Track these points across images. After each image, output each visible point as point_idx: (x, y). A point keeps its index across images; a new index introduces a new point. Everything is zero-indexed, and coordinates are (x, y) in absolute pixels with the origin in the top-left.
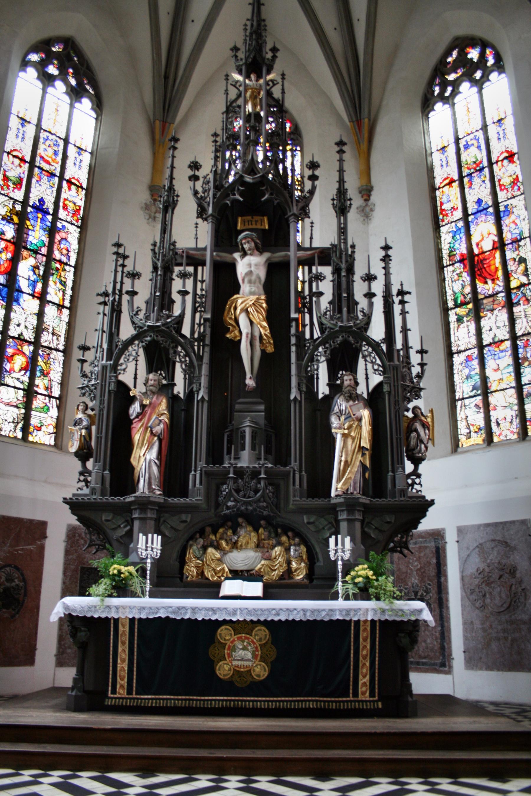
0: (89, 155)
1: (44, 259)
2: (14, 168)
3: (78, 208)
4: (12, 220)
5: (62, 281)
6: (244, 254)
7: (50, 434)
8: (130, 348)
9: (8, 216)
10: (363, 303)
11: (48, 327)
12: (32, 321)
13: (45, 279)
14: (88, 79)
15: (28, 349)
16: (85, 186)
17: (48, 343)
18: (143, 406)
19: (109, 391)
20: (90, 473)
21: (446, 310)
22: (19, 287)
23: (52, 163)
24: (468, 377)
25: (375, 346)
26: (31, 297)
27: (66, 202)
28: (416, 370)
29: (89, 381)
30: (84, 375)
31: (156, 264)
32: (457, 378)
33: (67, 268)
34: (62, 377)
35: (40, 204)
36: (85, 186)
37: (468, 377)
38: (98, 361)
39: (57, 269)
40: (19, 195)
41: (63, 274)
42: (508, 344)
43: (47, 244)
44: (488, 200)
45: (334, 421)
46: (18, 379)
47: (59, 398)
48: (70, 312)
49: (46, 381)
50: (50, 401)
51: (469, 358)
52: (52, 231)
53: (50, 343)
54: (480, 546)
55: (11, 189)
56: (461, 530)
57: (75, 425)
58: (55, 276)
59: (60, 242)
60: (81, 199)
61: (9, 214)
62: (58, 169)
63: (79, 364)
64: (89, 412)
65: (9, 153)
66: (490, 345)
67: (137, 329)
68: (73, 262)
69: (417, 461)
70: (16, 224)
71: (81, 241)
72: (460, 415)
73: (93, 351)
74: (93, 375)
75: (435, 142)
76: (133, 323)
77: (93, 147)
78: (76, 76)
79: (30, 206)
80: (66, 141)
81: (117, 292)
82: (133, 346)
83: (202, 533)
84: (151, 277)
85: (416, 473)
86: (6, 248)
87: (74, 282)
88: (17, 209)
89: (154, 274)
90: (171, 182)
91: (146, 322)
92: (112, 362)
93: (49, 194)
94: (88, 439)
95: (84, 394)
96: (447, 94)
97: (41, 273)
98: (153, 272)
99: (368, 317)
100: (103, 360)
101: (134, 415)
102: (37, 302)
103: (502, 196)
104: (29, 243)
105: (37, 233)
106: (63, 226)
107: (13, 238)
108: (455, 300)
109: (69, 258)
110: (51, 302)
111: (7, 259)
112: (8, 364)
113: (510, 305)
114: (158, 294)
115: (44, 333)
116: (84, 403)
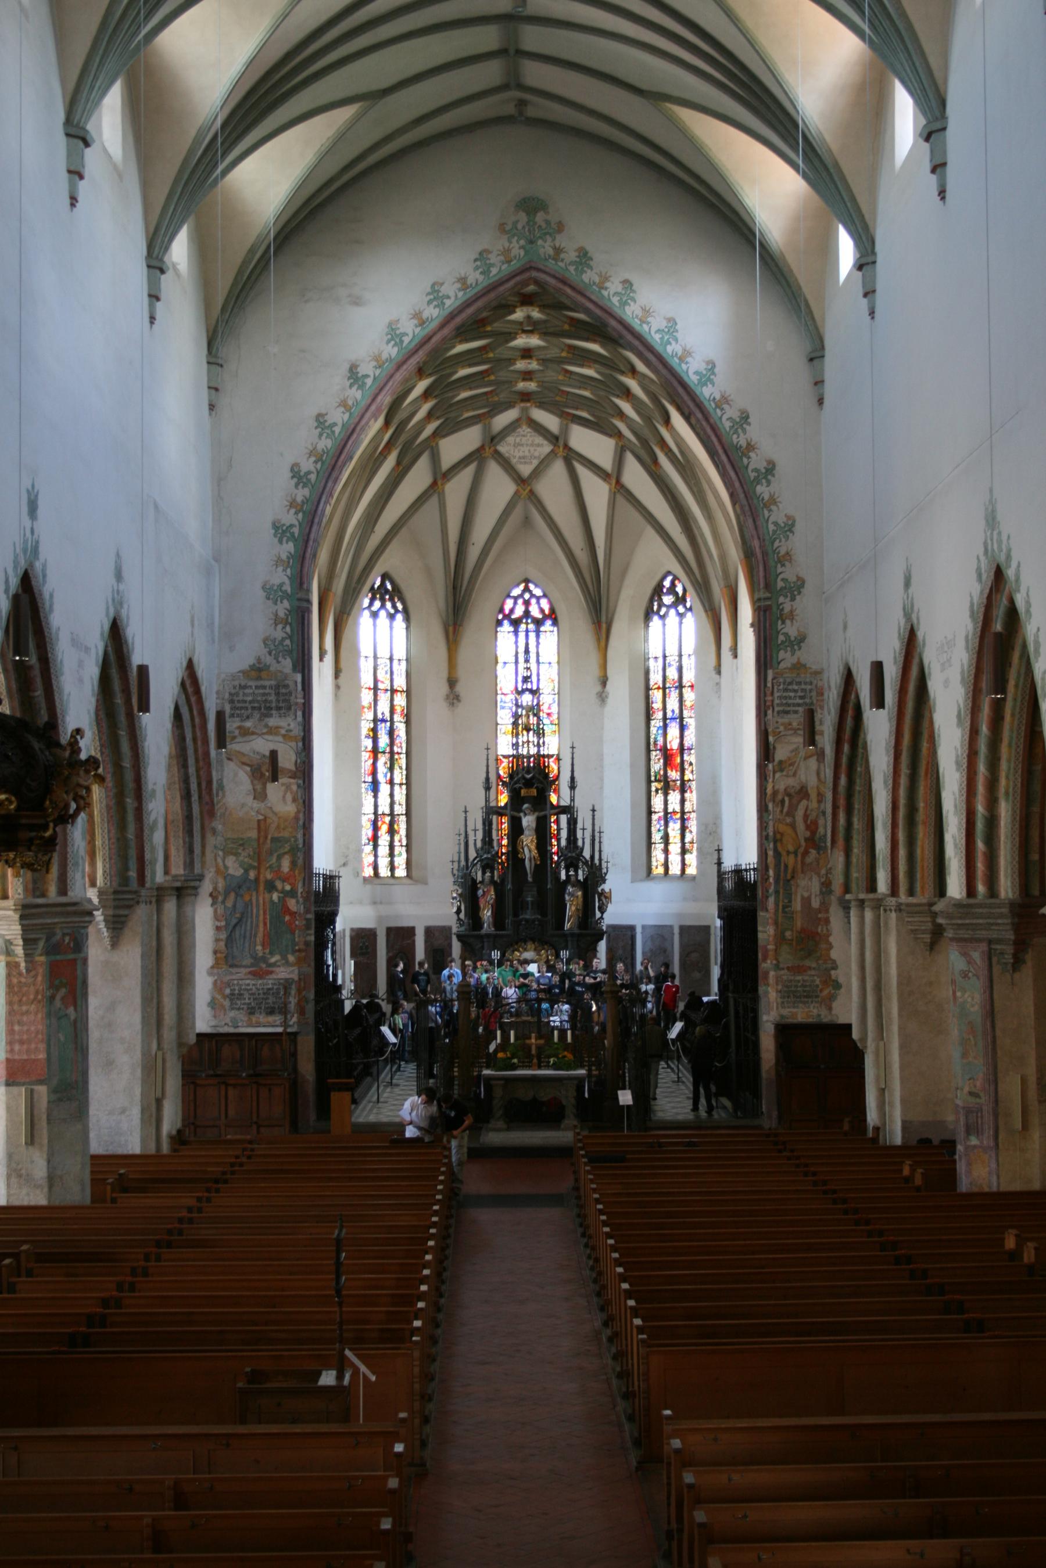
6: (525, 815)
10: (580, 843)
13: (391, 769)
15: (387, 819)
18: (484, 892)
20: (462, 920)
21: (649, 782)
24: (659, 830)
25: (586, 863)
28: (604, 871)
32: (653, 829)
37: (659, 830)
40: (370, 716)
42: (678, 816)
44: (677, 711)
45: (567, 897)
47: (407, 846)
51: (660, 819)
52: (391, 733)
54: (652, 937)
56: (644, 927)
66: (671, 813)
68: (404, 751)
69: (602, 913)
72: (653, 854)
75: (654, 648)
78: (392, 600)
80: (391, 659)
83: (512, 945)
85: (602, 918)
96: (662, 613)
99: (582, 849)
102: (388, 786)
103: (686, 713)
108: (656, 777)
109: (401, 747)
113: (683, 791)
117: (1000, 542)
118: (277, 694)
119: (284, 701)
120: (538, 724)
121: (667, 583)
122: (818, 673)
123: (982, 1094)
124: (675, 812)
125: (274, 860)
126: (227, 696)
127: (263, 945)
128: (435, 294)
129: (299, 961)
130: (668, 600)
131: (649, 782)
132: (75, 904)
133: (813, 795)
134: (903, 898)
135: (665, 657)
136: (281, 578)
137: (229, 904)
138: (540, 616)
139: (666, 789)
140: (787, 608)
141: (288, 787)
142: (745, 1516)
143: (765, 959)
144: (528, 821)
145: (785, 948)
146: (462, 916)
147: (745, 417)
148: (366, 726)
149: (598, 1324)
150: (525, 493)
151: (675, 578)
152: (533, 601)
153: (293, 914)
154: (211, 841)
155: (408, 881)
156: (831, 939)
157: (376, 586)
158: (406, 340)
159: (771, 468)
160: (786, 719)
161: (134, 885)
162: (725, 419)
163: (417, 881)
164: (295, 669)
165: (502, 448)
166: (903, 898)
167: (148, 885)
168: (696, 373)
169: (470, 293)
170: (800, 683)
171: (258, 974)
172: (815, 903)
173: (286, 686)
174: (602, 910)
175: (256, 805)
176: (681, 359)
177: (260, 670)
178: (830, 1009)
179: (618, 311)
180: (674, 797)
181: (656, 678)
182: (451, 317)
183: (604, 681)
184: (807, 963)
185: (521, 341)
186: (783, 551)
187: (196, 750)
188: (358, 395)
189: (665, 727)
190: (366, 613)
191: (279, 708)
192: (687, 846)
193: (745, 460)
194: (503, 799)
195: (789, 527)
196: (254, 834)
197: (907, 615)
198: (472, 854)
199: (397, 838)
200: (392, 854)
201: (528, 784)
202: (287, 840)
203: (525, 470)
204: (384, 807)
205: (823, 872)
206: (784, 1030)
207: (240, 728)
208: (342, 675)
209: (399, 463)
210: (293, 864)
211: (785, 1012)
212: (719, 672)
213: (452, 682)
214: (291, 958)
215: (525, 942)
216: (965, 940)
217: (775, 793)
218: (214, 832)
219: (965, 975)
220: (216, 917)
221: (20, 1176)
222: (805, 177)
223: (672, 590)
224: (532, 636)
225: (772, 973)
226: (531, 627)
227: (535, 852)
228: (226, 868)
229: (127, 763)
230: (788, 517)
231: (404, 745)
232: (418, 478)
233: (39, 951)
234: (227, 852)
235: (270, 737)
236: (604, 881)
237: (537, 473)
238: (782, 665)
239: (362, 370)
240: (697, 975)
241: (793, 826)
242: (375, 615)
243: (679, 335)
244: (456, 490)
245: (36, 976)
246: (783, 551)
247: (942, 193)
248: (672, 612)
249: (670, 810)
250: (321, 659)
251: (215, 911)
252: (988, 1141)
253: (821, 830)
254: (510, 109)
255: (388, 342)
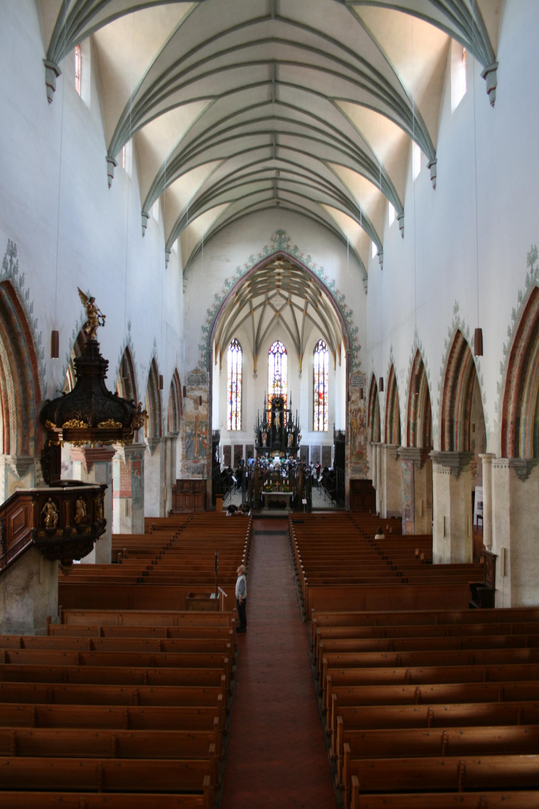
10: (293, 421)
13: (236, 397)
21: (314, 402)
25: (294, 427)
32: (315, 417)
44: (322, 382)
52: (236, 386)
56: (311, 446)
75: (316, 363)
78: (237, 346)
103: (325, 382)
113: (324, 405)
117: (418, 342)
118: (202, 378)
119: (204, 380)
120: (281, 384)
121: (320, 343)
122: (364, 374)
123: (410, 505)
124: (321, 412)
125: (200, 428)
126: (187, 378)
127: (197, 453)
128: (251, 259)
129: (208, 458)
130: (320, 348)
131: (314, 402)
132: (140, 445)
133: (362, 411)
134: (388, 444)
135: (319, 365)
136: (204, 343)
137: (187, 441)
138: (282, 352)
139: (319, 404)
140: (355, 355)
141: (205, 406)
142: (335, 643)
143: (347, 460)
144: (277, 414)
145: (353, 457)
146: (257, 442)
147: (344, 297)
148: (229, 384)
149: (294, 574)
150: (278, 315)
151: (323, 341)
152: (280, 347)
153: (206, 444)
154: (182, 422)
155: (241, 431)
156: (367, 454)
157: (233, 342)
158: (242, 272)
159: (351, 313)
160: (355, 388)
161: (158, 437)
162: (338, 297)
163: (243, 431)
164: (207, 370)
165: (271, 301)
166: (388, 444)
167: (162, 436)
168: (329, 283)
169: (262, 258)
170: (359, 377)
171: (195, 462)
172: (362, 443)
173: (205, 376)
174: (299, 441)
175: (195, 411)
176: (325, 279)
177: (197, 371)
178: (366, 475)
179: (306, 265)
180: (321, 407)
181: (316, 371)
182: (256, 265)
183: (301, 372)
184: (360, 461)
185: (277, 271)
186: (354, 337)
187: (177, 395)
188: (228, 288)
189: (319, 386)
191: (202, 382)
192: (325, 422)
193: (344, 310)
194: (270, 407)
195: (356, 330)
196: (194, 420)
197: (391, 360)
198: (260, 424)
199: (238, 418)
200: (236, 423)
201: (277, 403)
202: (204, 422)
203: (278, 308)
204: (234, 409)
205: (365, 434)
206: (352, 482)
207: (191, 388)
208: (222, 369)
209: (240, 306)
210: (206, 429)
211: (353, 476)
212: (335, 370)
213: (255, 371)
214: (205, 457)
215: (276, 450)
216: (406, 460)
217: (351, 410)
218: (183, 419)
219: (406, 470)
220: (183, 445)
221: (123, 525)
222: (362, 227)
223: (322, 345)
224: (279, 357)
225: (349, 464)
226: (279, 355)
227: (279, 423)
228: (186, 430)
229: (157, 401)
230: (356, 327)
232: (246, 310)
233: (130, 458)
234: (186, 425)
235: (200, 391)
236: (300, 432)
237: (281, 309)
238: (354, 372)
239: (229, 281)
240: (327, 461)
241: (356, 420)
242: (232, 351)
243: (324, 272)
244: (257, 314)
245: (129, 466)
246: (354, 337)
247: (403, 236)
248: (322, 351)
249: (320, 411)
250: (216, 364)
251: (183, 443)
252: (411, 519)
253: (365, 421)
254: (275, 204)
255: (237, 273)
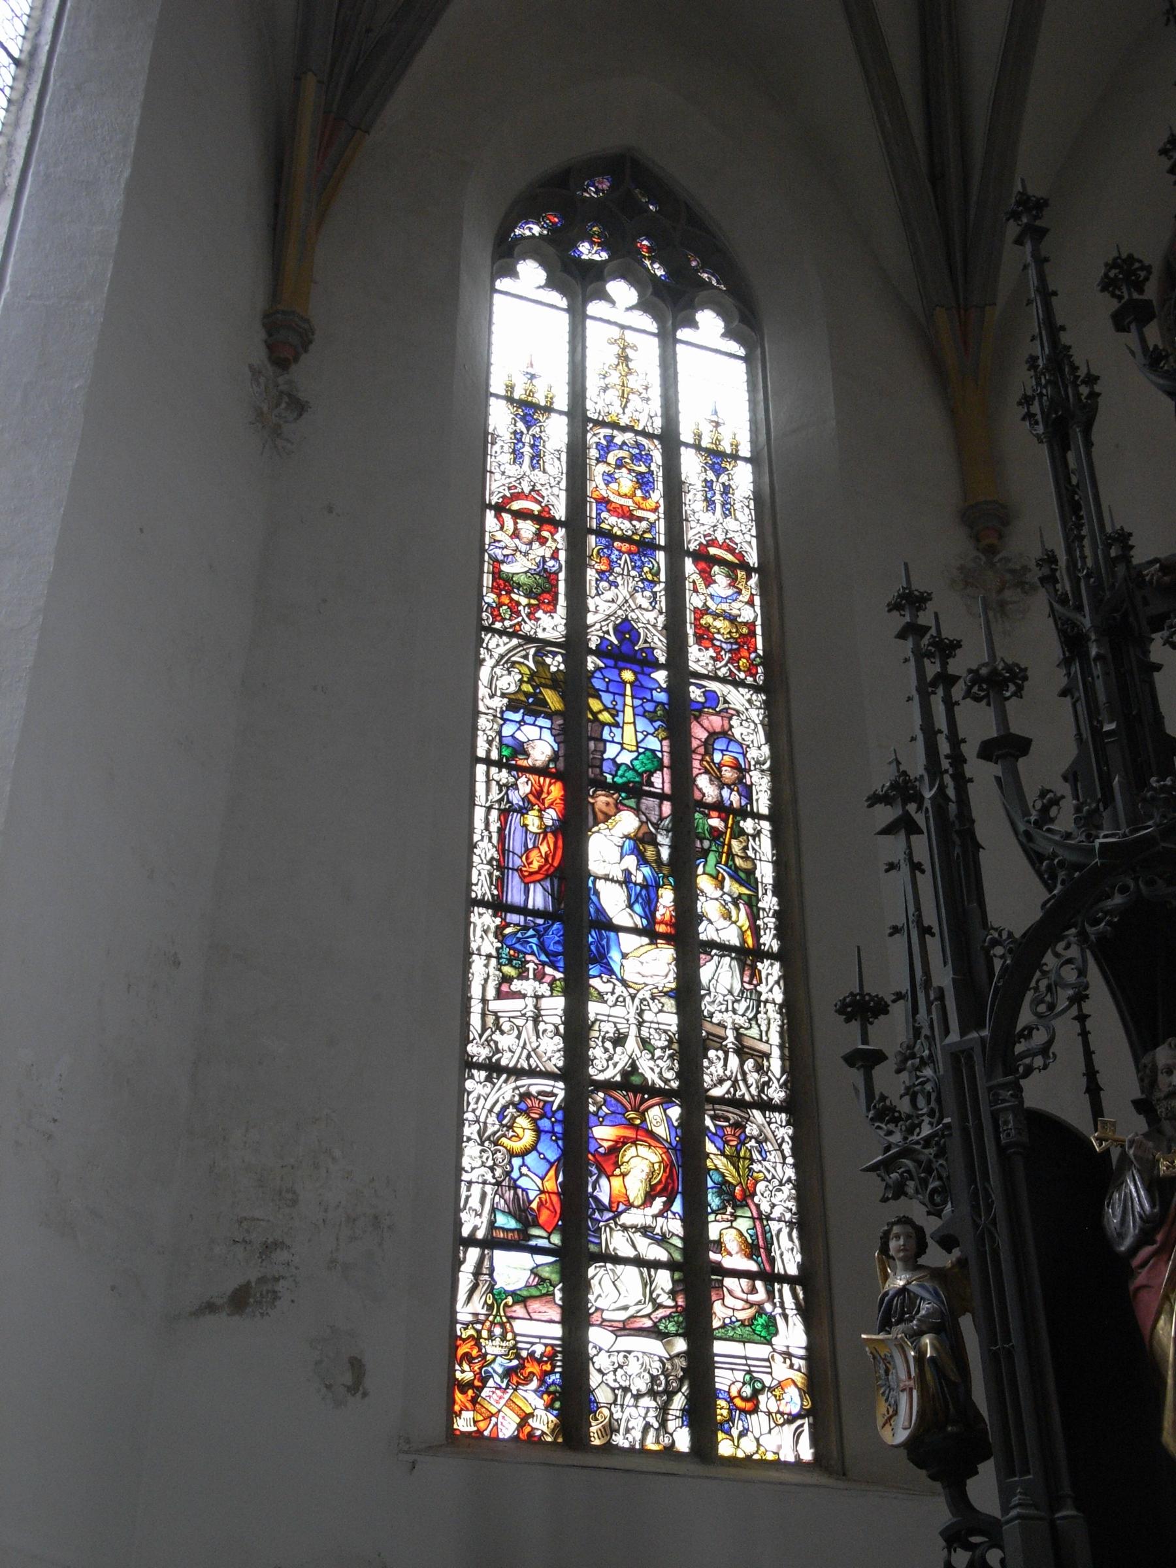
0: (749, 467)
1: (667, 808)
2: (524, 548)
3: (745, 630)
4: (545, 703)
5: (737, 869)
7: (792, 1418)
8: (1049, 960)
9: (528, 695)
11: (719, 1031)
12: (662, 1017)
14: (697, 254)
16: (753, 559)
17: (728, 1084)
19: (1001, 1150)
20: (992, 1530)
22: (600, 911)
23: (639, 513)
26: (645, 940)
27: (707, 619)
29: (910, 1131)
30: (884, 1114)
31: (1074, 625)
33: (748, 825)
34: (800, 1199)
35: (621, 639)
36: (753, 559)
38: (931, 1039)
39: (716, 835)
41: (736, 846)
43: (666, 761)
46: (646, 1231)
47: (802, 1279)
48: (783, 967)
49: (743, 1224)
50: (770, 1294)
53: (735, 1082)
55: (524, 612)
57: (885, 1325)
58: (712, 858)
59: (708, 746)
60: (751, 603)
61: (527, 688)
62: (661, 526)
63: (856, 1076)
64: (936, 1257)
65: (499, 509)
67: (1062, 875)
70: (557, 713)
71: (773, 731)
73: (899, 1010)
74: (921, 1101)
76: (1035, 858)
77: (754, 442)
79: (592, 652)
80: (669, 439)
81: (945, 764)
82: (1060, 947)
84: (1064, 681)
86: (538, 793)
87: (779, 864)
88: (553, 669)
89: (1076, 668)
90: (1054, 342)
91: (1090, 837)
92: (985, 1033)
93: (646, 604)
94: (954, 1376)
95: (899, 1191)
97: (665, 853)
98: (1067, 662)
100: (947, 1032)
101: (1132, 1231)
104: (607, 766)
105: (629, 729)
106: (710, 695)
107: (555, 758)
109: (747, 792)
110: (712, 944)
111: (545, 830)
112: (604, 1181)
114: (1109, 727)
115: (712, 1054)
116: (905, 1221)
190: (531, 273)
231: (761, 785)
